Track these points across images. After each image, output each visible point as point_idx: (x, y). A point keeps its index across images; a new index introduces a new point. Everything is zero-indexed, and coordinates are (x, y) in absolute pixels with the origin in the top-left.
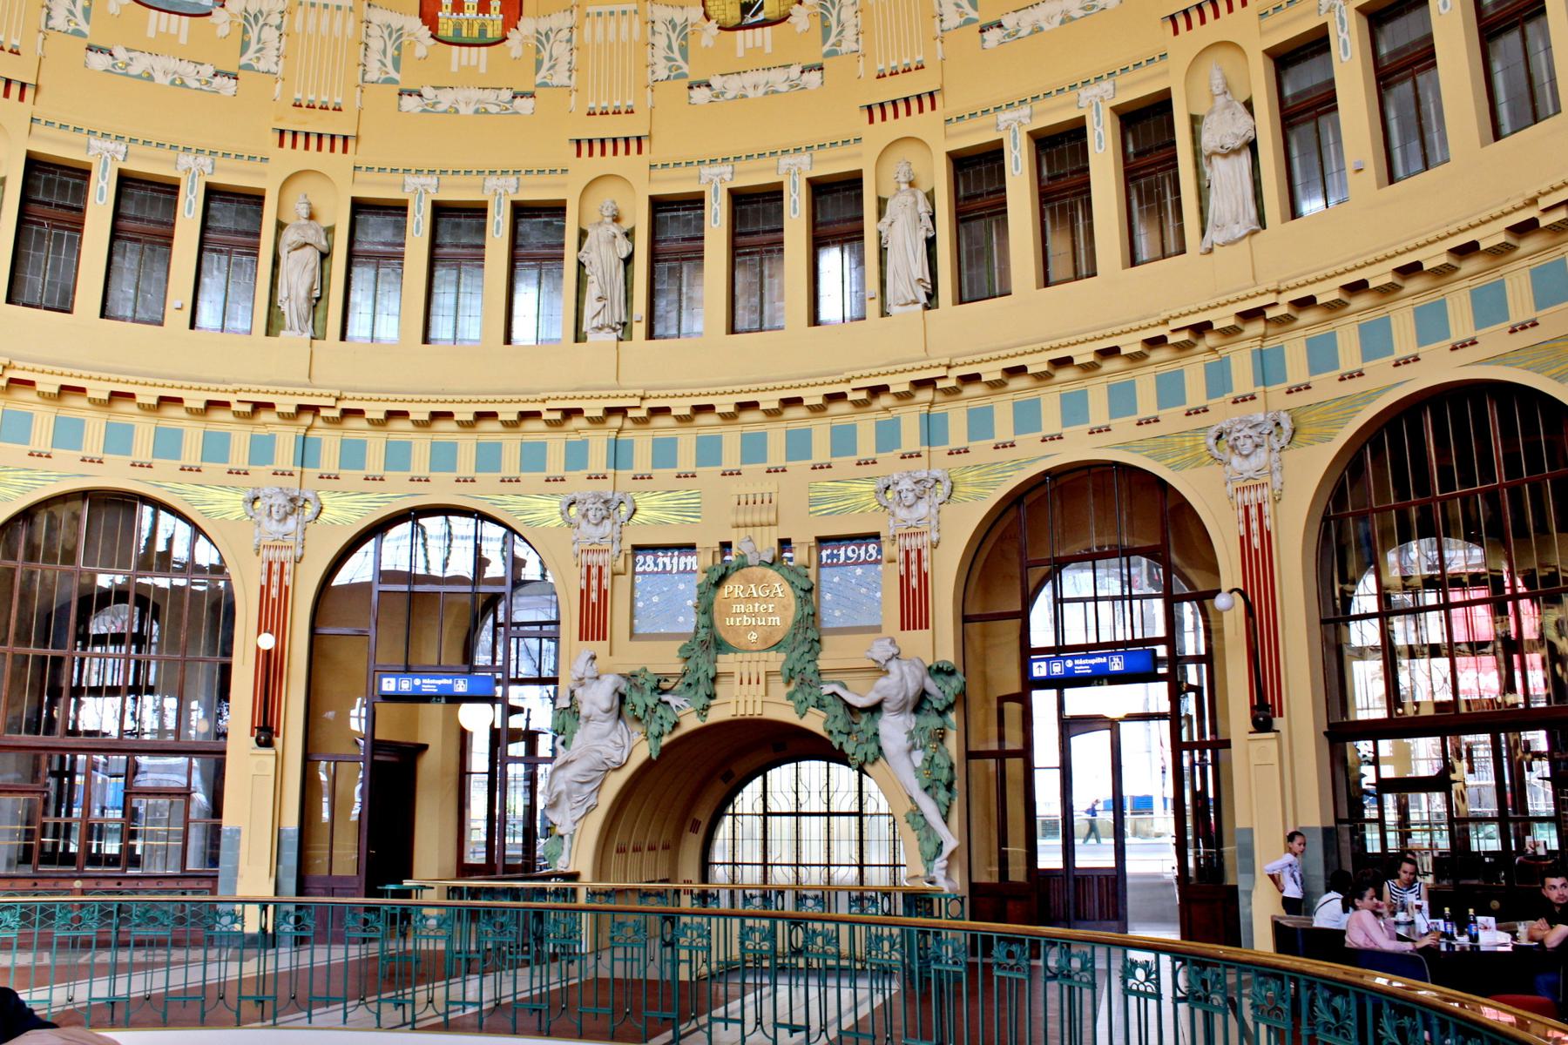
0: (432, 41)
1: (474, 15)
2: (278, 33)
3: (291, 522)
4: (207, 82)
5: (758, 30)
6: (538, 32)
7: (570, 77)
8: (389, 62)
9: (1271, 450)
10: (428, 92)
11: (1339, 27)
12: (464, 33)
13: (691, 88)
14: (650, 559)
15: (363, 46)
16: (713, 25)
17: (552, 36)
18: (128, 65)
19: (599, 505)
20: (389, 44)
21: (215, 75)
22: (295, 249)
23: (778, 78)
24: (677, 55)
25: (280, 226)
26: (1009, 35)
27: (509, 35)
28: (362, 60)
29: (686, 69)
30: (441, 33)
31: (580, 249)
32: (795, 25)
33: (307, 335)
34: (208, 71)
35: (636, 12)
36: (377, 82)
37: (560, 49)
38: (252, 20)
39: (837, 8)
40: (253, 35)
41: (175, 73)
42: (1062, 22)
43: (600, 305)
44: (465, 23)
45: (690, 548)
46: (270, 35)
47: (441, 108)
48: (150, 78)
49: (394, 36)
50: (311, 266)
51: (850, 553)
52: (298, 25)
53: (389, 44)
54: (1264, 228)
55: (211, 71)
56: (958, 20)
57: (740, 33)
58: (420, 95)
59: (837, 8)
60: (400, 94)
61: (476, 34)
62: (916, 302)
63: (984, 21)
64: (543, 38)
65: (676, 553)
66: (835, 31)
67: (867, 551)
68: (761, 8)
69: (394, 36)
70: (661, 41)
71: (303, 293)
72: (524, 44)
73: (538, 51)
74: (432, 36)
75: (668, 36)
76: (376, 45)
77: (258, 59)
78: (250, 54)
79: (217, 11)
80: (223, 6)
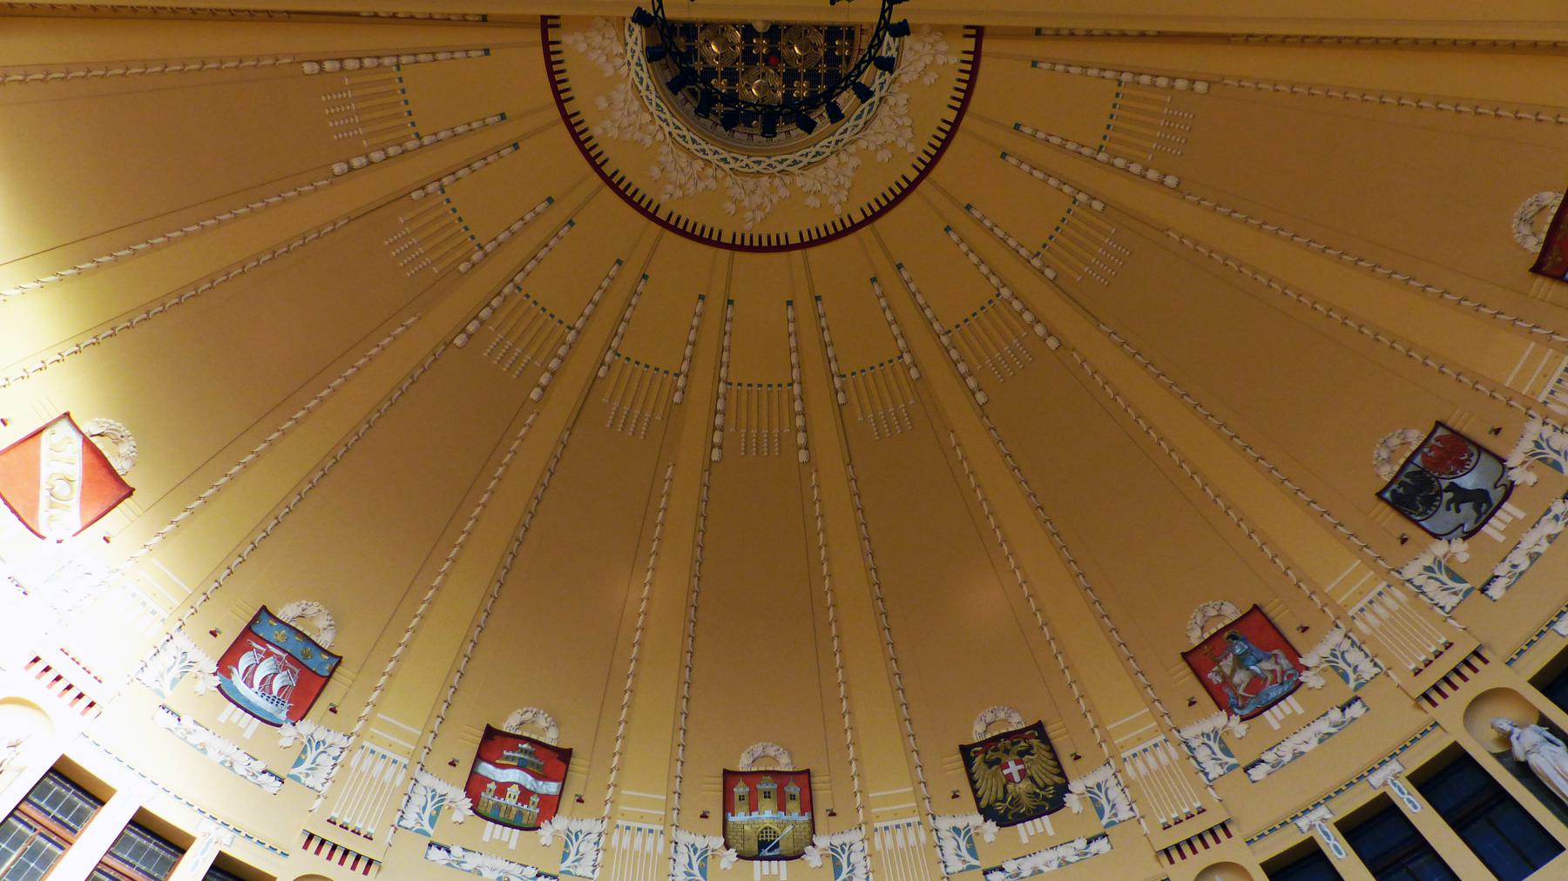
0: (471, 812)
1: (514, 802)
2: (333, 762)
4: (254, 775)
5: (774, 863)
6: (569, 830)
7: (593, 871)
8: (426, 817)
10: (457, 851)
11: (1325, 838)
12: (502, 815)
15: (407, 797)
16: (732, 853)
17: (581, 837)
18: (190, 733)
20: (430, 804)
21: (264, 772)
24: (696, 871)
26: (1011, 877)
27: (542, 825)
28: (403, 808)
30: (481, 809)
32: (808, 862)
34: (260, 766)
36: (411, 829)
37: (587, 848)
38: (314, 745)
39: (847, 853)
40: (310, 756)
41: (228, 756)
42: (1060, 866)
44: (505, 807)
46: (326, 761)
47: (465, 866)
48: (204, 751)
49: (436, 799)
52: (354, 762)
53: (430, 804)
55: (262, 767)
56: (961, 866)
57: (757, 863)
58: (449, 851)
59: (847, 853)
60: (430, 845)
61: (512, 817)
63: (987, 867)
64: (572, 836)
66: (845, 869)
68: (777, 845)
69: (436, 799)
70: (683, 859)
72: (554, 836)
73: (566, 846)
74: (471, 809)
75: (690, 857)
76: (418, 800)
77: (307, 775)
78: (302, 769)
79: (287, 727)
80: (294, 725)
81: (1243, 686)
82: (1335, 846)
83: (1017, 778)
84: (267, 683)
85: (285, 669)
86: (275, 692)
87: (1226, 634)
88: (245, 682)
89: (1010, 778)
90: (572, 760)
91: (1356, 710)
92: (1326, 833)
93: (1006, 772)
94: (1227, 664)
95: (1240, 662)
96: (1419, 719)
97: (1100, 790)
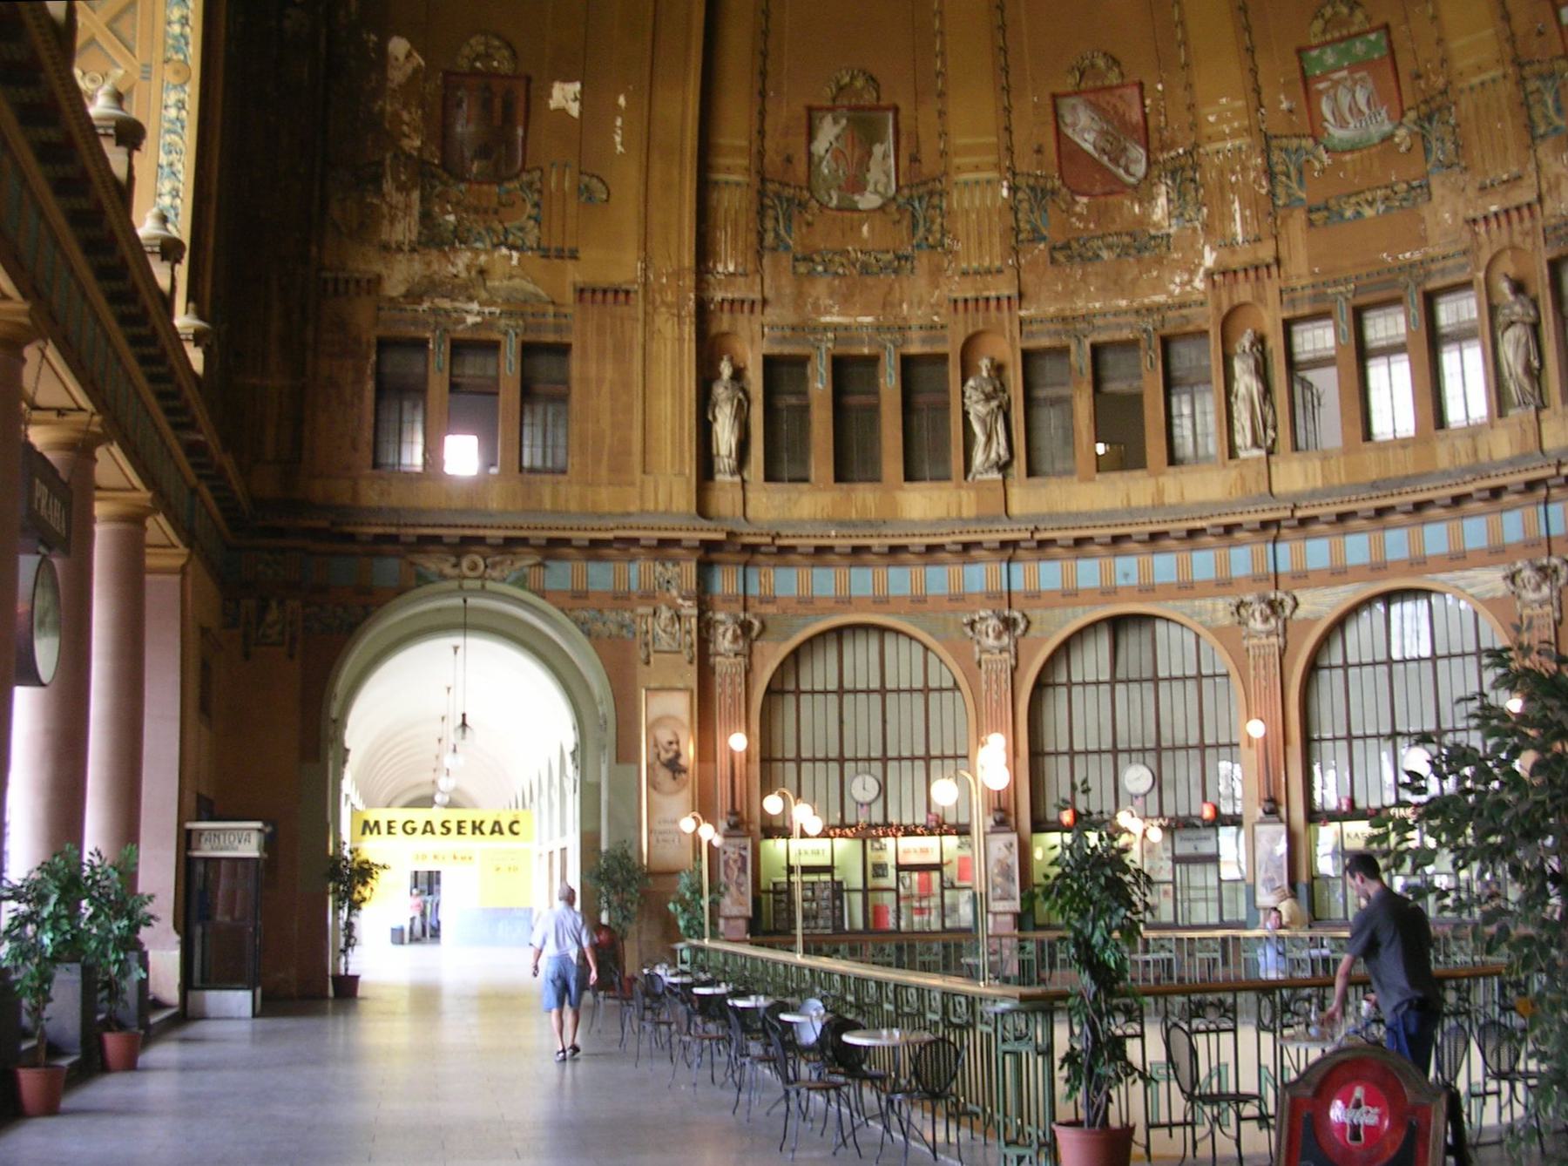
3: (1546, 590)
33: (1532, 408)
50: (1523, 340)
84: (1355, 110)
85: (1355, 83)
86: (1364, 108)
88: (1341, 127)
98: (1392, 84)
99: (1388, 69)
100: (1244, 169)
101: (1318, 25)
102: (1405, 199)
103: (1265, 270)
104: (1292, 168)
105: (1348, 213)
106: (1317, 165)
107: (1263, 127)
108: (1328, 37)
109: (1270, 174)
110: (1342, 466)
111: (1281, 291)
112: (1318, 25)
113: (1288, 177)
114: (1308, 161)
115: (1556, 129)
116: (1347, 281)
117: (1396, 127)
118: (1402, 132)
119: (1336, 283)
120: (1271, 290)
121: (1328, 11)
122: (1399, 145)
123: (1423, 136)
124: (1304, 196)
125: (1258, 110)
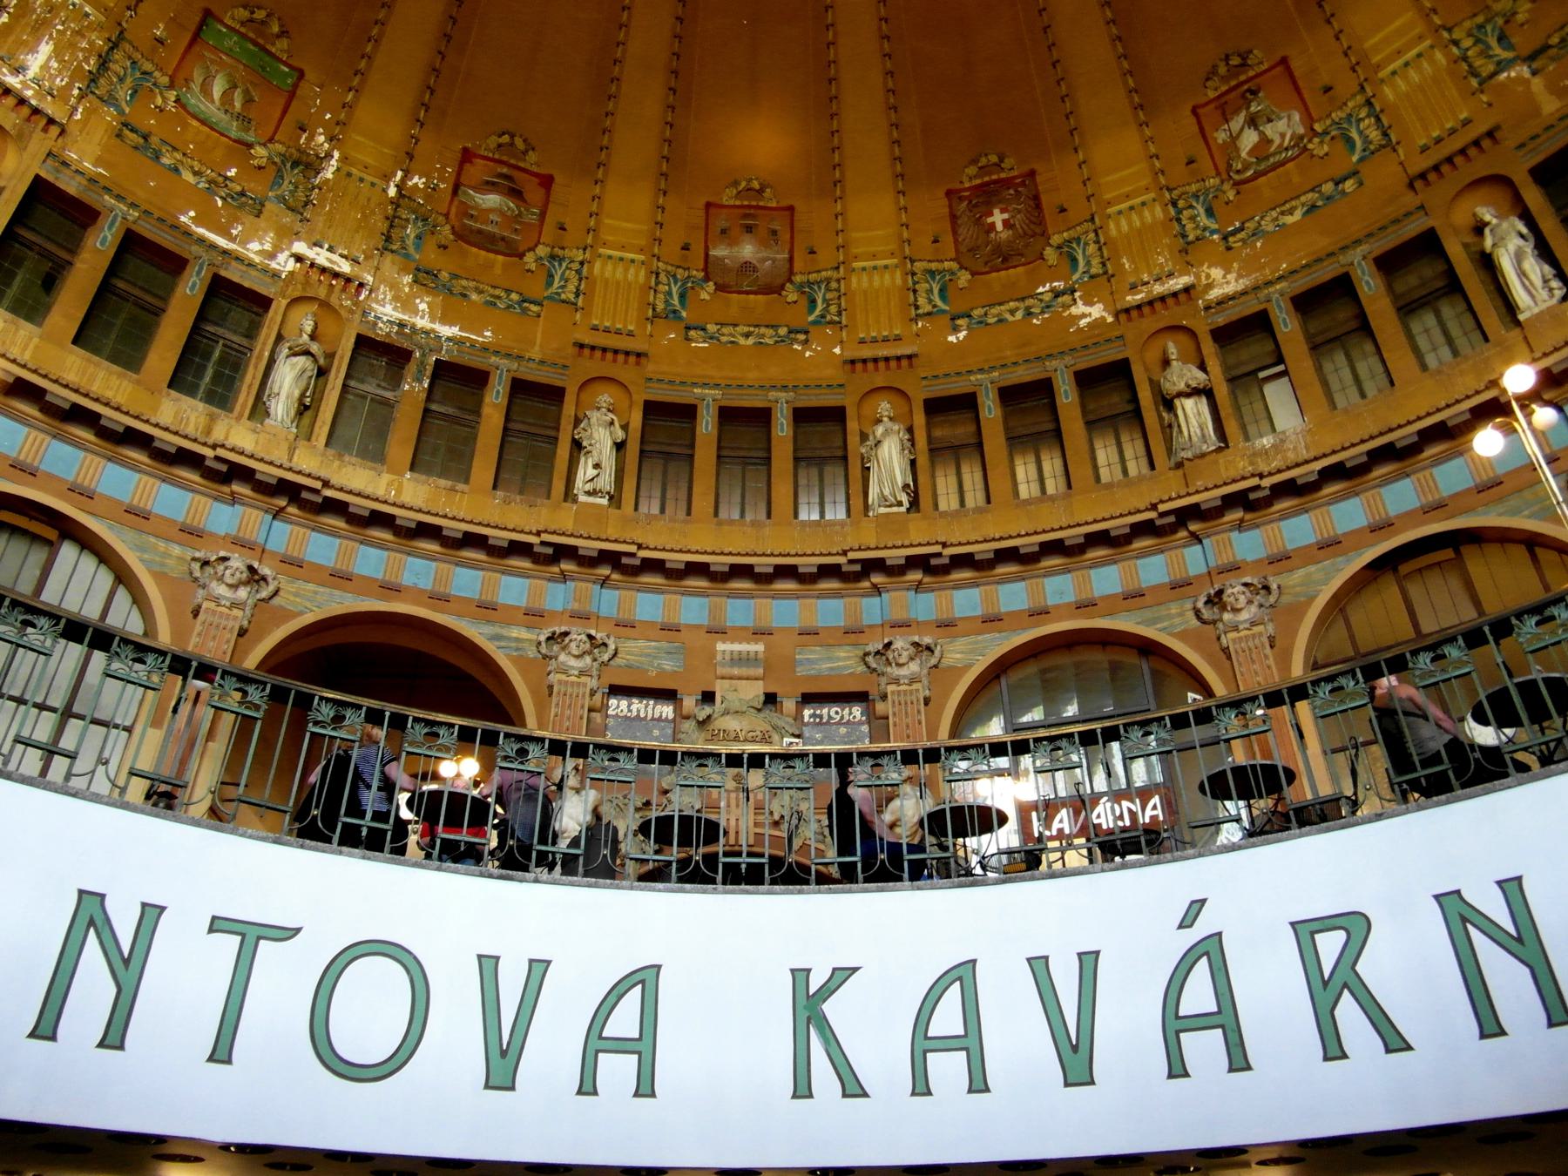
3: (243, 593)
9: (1261, 606)
13: (688, 328)
14: (624, 703)
16: (711, 286)
19: (584, 637)
22: (295, 355)
23: (769, 337)
25: (280, 338)
29: (684, 314)
31: (576, 426)
35: (643, 263)
43: (595, 472)
45: (667, 695)
50: (310, 374)
51: (832, 714)
54: (1227, 446)
62: (900, 504)
65: (652, 702)
67: (850, 714)
71: (297, 393)
81: (1247, 149)
82: (1284, 320)
83: (999, 227)
87: (1246, 87)
89: (993, 225)
90: (555, 188)
91: (1349, 185)
92: (1279, 306)
93: (990, 220)
94: (1238, 122)
95: (1252, 122)
96: (1410, 200)
97: (1078, 245)
98: (278, 114)
99: (282, 101)
100: (79, 33)
101: (243, 14)
102: (232, 197)
103: (44, 121)
104: (129, 80)
105: (166, 161)
106: (159, 101)
107: (124, 24)
108: (243, 30)
109: (104, 63)
110: (31, 346)
111: (49, 155)
112: (243, 14)
113: (121, 80)
114: (151, 90)
115: (407, 256)
116: (133, 205)
117: (260, 144)
118: (260, 151)
119: (119, 198)
120: (40, 142)
121: (260, 15)
122: (255, 158)
123: (279, 170)
124: (127, 110)
125: (129, 8)
